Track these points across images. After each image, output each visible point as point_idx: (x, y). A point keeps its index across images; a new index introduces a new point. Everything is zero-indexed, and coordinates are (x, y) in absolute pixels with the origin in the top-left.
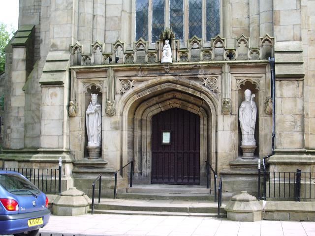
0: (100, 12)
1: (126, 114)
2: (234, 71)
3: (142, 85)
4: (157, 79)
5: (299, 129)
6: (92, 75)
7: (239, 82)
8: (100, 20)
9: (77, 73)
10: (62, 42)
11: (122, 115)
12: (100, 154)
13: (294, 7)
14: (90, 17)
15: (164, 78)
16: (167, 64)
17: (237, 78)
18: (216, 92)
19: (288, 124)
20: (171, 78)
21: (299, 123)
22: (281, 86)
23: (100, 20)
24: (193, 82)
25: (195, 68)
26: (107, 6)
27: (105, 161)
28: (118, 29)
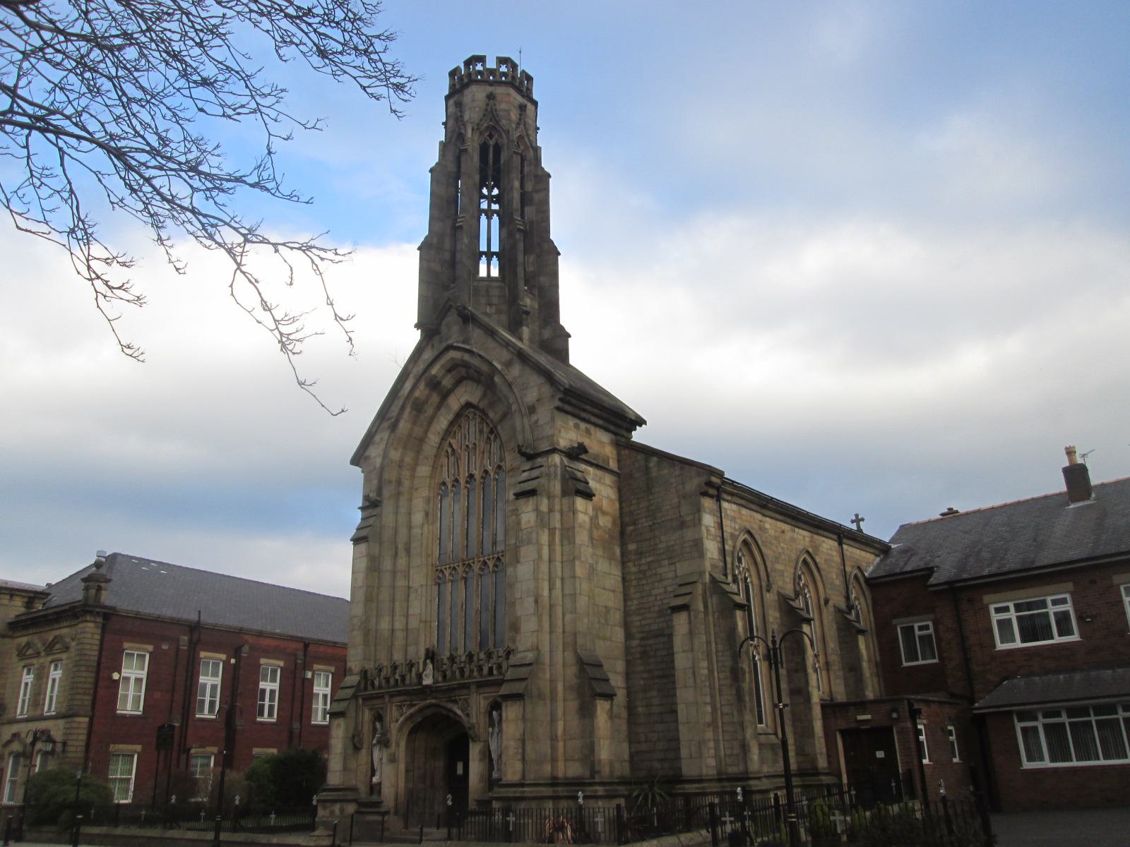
0: (399, 625)
1: (403, 744)
2: (482, 690)
3: (412, 710)
4: (423, 704)
5: (519, 757)
6: (376, 702)
7: (487, 702)
8: (400, 635)
9: (364, 699)
10: (356, 666)
11: (398, 745)
12: (380, 792)
13: (532, 611)
15: (428, 701)
16: (427, 686)
17: (485, 698)
18: (468, 715)
19: (511, 752)
20: (433, 701)
21: (520, 750)
22: (506, 707)
23: (400, 635)
24: (450, 705)
25: (451, 690)
26: (410, 618)
27: (383, 799)
28: (417, 644)
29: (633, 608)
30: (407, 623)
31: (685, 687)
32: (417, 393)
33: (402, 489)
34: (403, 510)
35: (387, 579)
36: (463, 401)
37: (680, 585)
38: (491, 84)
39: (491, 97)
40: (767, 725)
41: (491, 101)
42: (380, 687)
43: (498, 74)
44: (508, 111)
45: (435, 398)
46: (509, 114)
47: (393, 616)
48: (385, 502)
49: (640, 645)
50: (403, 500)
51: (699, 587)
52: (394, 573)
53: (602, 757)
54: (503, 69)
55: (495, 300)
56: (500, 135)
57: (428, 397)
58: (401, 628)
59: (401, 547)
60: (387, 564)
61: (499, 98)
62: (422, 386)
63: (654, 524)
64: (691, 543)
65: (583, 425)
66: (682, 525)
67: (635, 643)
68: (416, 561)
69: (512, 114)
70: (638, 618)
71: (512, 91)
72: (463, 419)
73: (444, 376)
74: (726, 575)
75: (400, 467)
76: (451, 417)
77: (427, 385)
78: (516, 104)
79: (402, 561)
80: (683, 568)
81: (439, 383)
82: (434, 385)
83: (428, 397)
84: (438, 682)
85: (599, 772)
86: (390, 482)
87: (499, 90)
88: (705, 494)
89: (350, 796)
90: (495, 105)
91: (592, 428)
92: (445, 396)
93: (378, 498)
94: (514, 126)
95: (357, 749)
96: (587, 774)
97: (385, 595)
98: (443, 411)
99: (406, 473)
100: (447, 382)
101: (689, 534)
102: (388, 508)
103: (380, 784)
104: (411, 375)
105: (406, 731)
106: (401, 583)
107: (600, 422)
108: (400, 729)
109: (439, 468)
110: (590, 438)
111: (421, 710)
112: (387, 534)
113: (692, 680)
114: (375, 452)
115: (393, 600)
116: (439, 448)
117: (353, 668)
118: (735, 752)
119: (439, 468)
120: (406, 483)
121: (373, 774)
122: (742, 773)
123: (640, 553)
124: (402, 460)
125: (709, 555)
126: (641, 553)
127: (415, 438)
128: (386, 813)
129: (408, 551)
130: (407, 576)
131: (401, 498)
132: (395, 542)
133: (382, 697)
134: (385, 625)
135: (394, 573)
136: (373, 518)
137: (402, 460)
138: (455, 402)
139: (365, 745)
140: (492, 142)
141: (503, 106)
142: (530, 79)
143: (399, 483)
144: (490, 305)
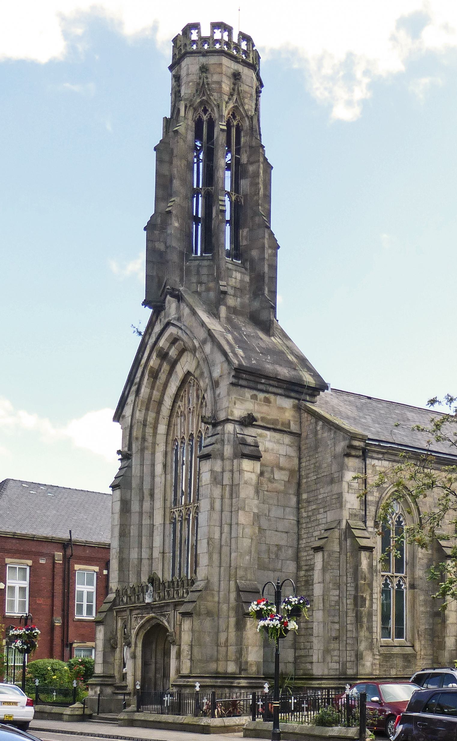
1: (140, 645)
9: (117, 612)
11: (136, 646)
14: (136, 562)
29: (303, 546)
30: (152, 554)
31: (319, 610)
32: (151, 363)
33: (146, 444)
34: (147, 462)
35: (135, 519)
36: (185, 370)
37: (325, 530)
38: (205, 54)
39: (204, 69)
40: (406, 639)
41: (204, 74)
42: (127, 603)
43: (211, 42)
44: (219, 83)
45: (166, 367)
46: (221, 87)
47: (141, 548)
48: (134, 455)
49: (305, 576)
50: (147, 454)
51: (336, 533)
52: (141, 513)
53: (250, 659)
54: (218, 35)
55: (204, 279)
56: (212, 110)
57: (161, 366)
58: (147, 557)
59: (146, 493)
60: (135, 507)
61: (212, 69)
62: (154, 356)
63: (317, 478)
64: (336, 496)
65: (261, 396)
66: (332, 481)
67: (302, 573)
68: (158, 504)
69: (224, 86)
70: (305, 554)
71: (225, 61)
72: (186, 386)
73: (170, 348)
74: (365, 522)
75: (145, 425)
76: (178, 383)
77: (158, 356)
78: (230, 72)
79: (147, 505)
80: (330, 516)
81: (167, 354)
82: (163, 356)
83: (161, 366)
84: (155, 601)
85: (246, 670)
86: (137, 439)
87: (212, 60)
88: (348, 455)
89: (110, 681)
90: (207, 78)
91: (272, 397)
92: (173, 365)
93: (129, 452)
94: (226, 98)
95: (114, 648)
96: (238, 671)
97: (134, 531)
98: (173, 377)
99: (149, 430)
100: (173, 353)
101: (335, 488)
102: (135, 460)
103: (126, 674)
104: (148, 346)
105: (141, 635)
106: (146, 521)
107: (279, 391)
108: (137, 634)
109: (173, 426)
110: (269, 406)
111: (148, 621)
112: (135, 483)
113: (321, 605)
114: (128, 411)
115: (140, 536)
116: (172, 409)
117: (113, 587)
118: (352, 659)
119: (173, 426)
120: (150, 439)
121: (124, 667)
122: (354, 675)
123: (308, 502)
124: (145, 420)
125: (348, 506)
126: (309, 502)
127: (154, 401)
128: (129, 694)
129: (152, 495)
130: (151, 516)
131: (146, 452)
132: (141, 489)
133: (126, 611)
134: (134, 555)
135: (141, 513)
136: (125, 469)
137: (145, 420)
138: (180, 371)
139: (119, 646)
140: (205, 118)
141: (216, 78)
142: (247, 38)
143: (144, 439)
144: (201, 283)
